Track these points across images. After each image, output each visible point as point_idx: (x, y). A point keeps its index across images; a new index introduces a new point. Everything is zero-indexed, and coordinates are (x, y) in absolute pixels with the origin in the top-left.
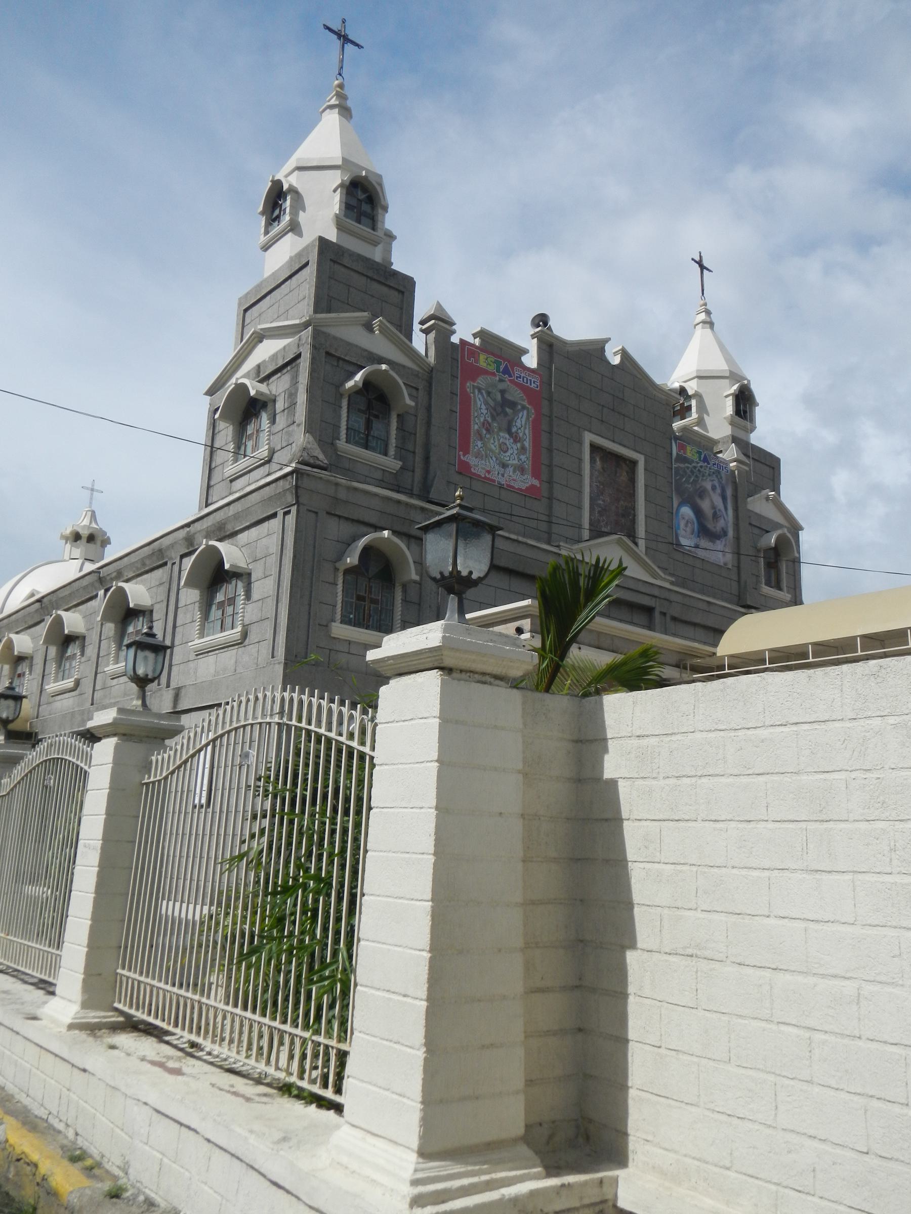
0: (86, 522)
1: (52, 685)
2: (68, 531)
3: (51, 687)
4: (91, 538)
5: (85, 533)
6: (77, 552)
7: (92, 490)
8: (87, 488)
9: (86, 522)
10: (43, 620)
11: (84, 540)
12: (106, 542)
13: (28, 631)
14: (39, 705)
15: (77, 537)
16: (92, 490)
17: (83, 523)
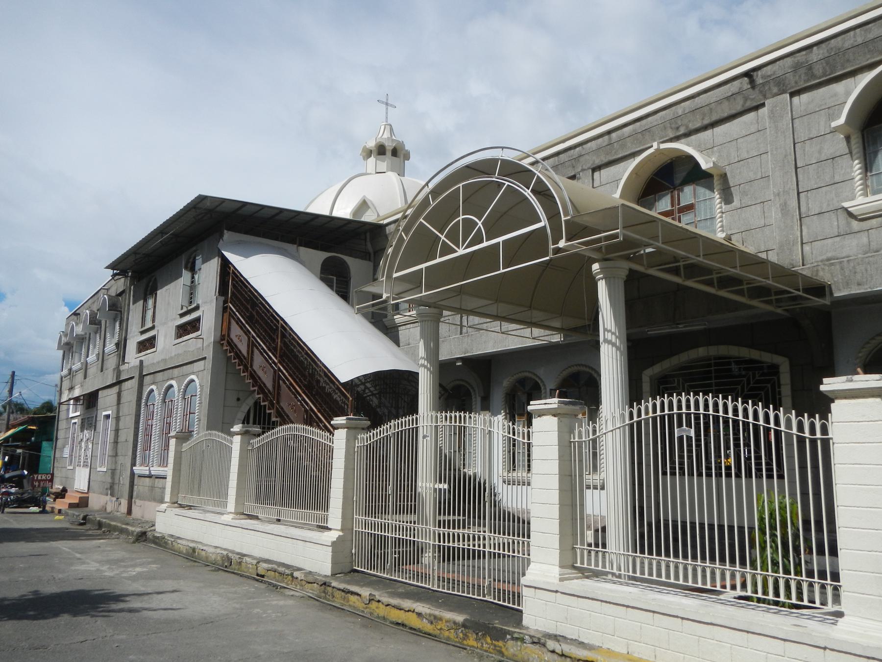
0: (387, 135)
1: (860, 200)
2: (372, 144)
3: (860, 203)
4: (395, 152)
5: (389, 145)
6: (383, 165)
7: (387, 104)
8: (383, 102)
9: (387, 135)
10: (763, 105)
11: (389, 153)
12: (407, 156)
13: (683, 141)
14: (802, 244)
15: (381, 150)
16: (387, 104)
17: (384, 136)
